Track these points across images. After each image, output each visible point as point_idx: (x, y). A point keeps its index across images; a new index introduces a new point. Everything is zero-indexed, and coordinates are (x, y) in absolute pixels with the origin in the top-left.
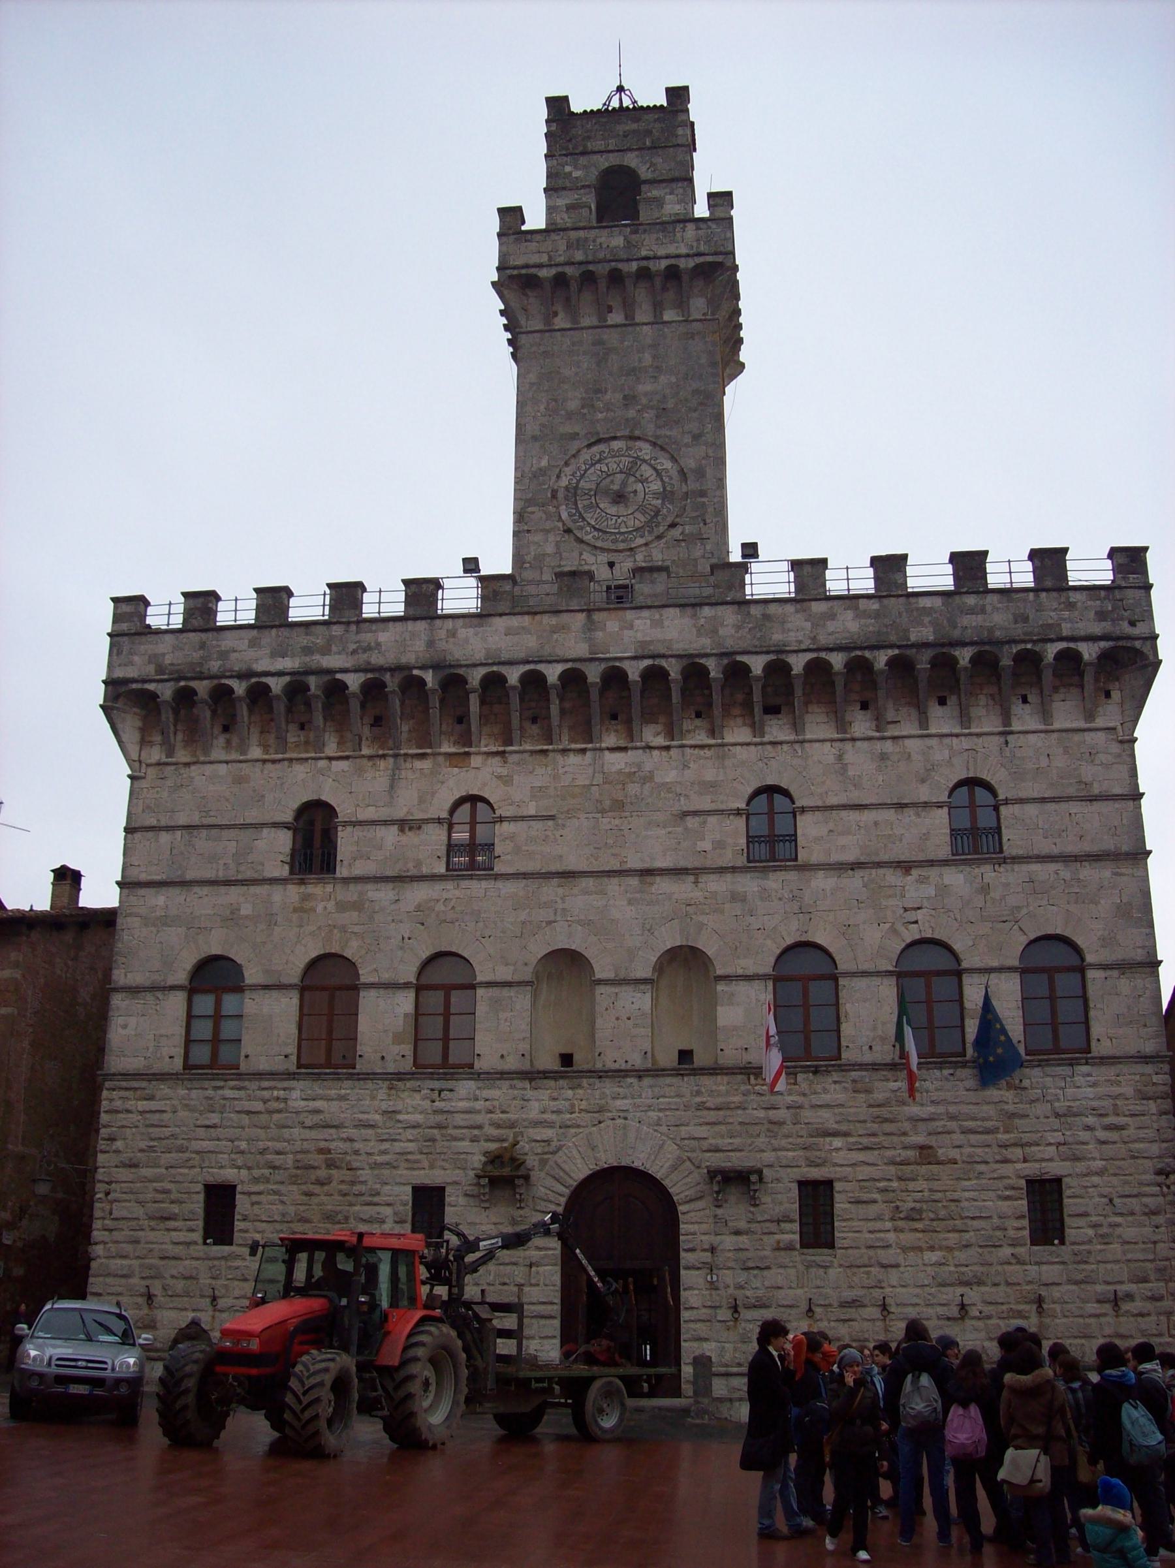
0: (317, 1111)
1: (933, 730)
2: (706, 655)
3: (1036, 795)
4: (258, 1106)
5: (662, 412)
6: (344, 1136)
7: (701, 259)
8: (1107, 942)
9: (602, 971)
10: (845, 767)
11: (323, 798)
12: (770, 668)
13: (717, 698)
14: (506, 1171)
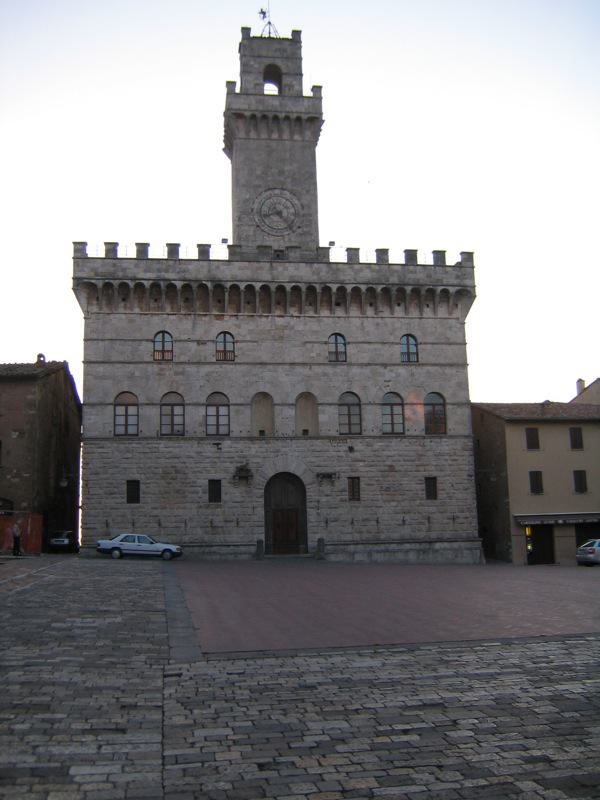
0: (170, 452)
4: (148, 451)
9: (277, 400)
10: (363, 328)
12: (338, 289)
13: (319, 298)
14: (243, 474)
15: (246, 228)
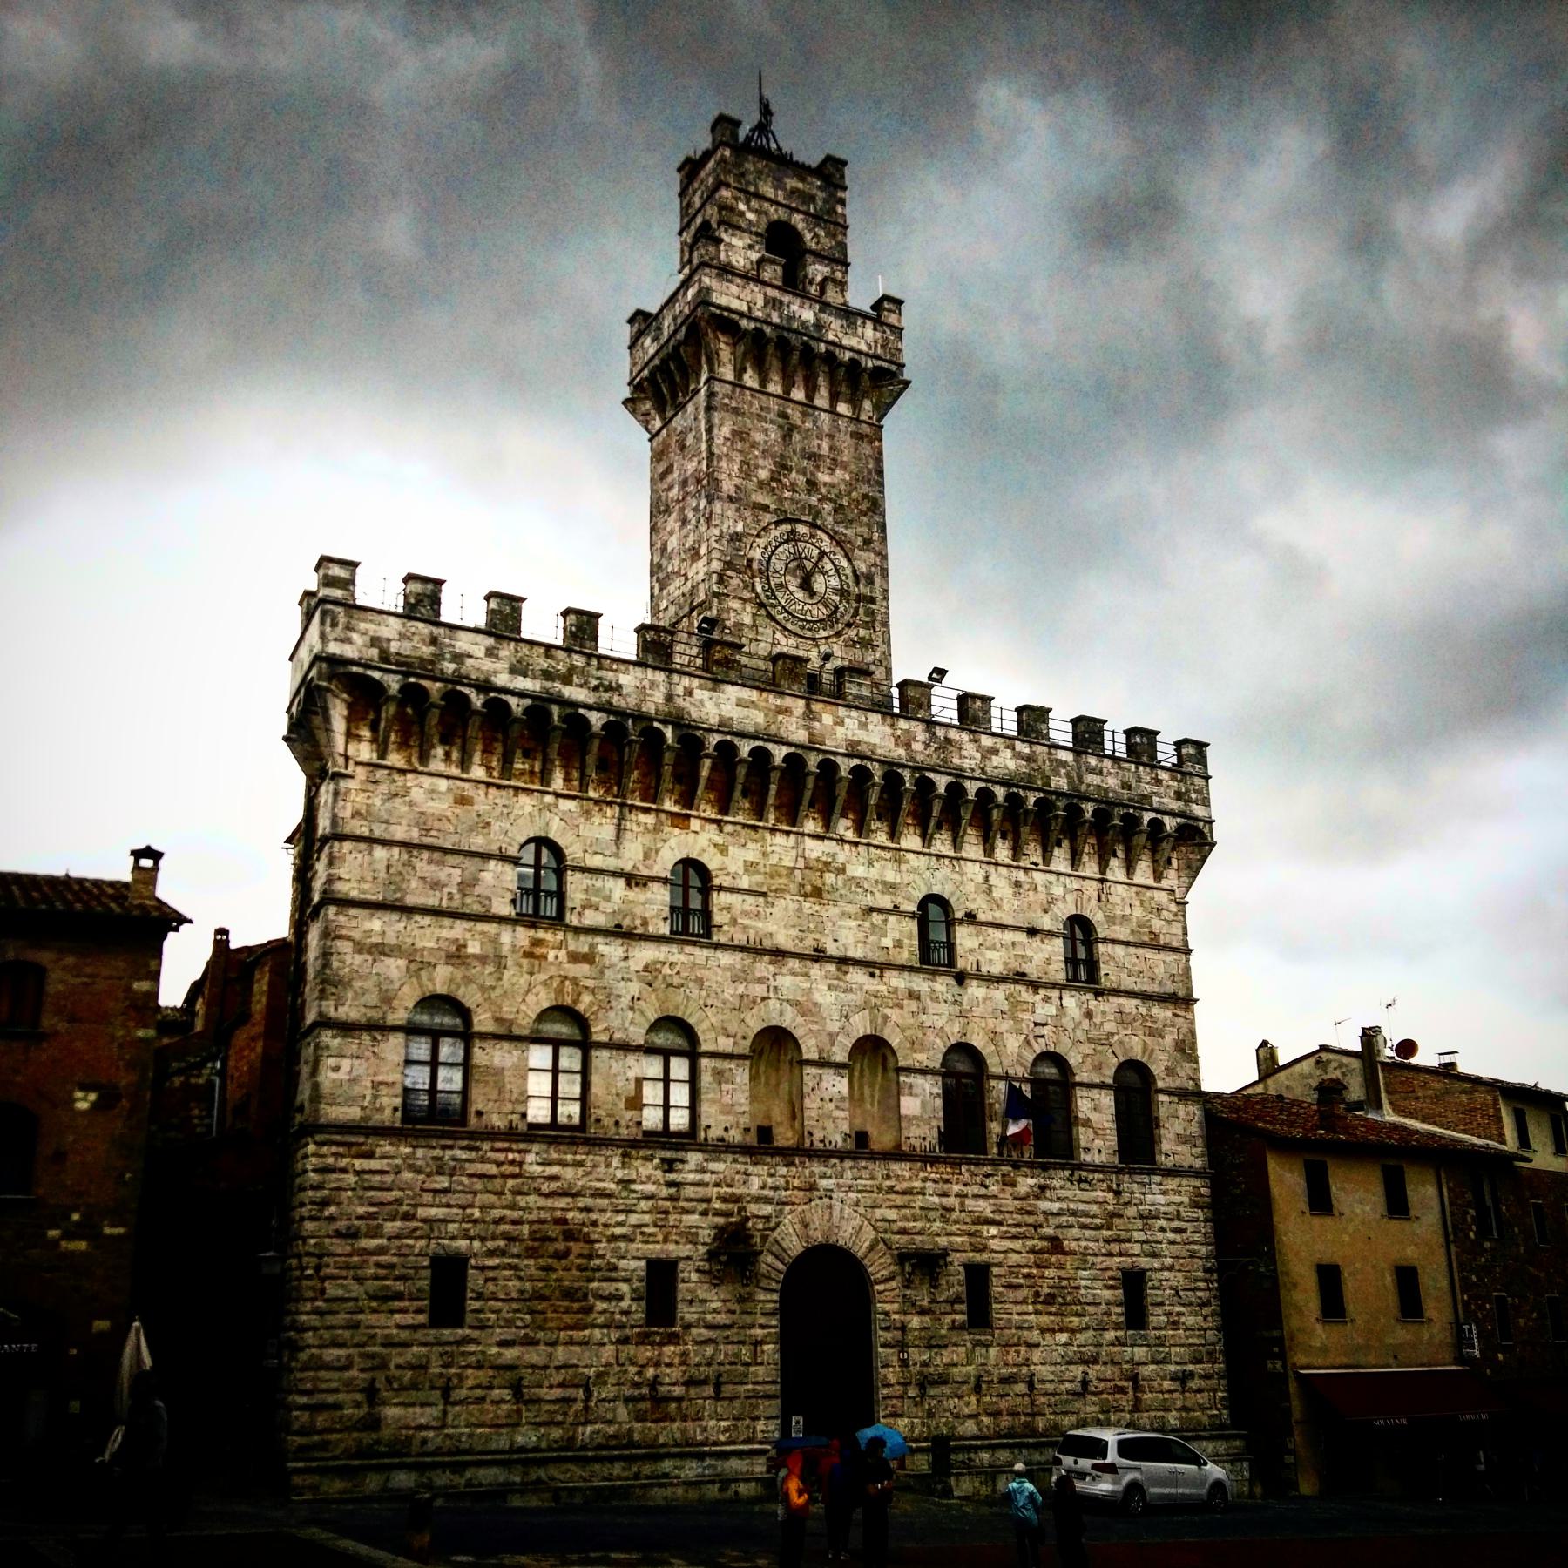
1: (1052, 867)
2: (904, 766)
3: (1122, 938)
4: (492, 1169)
5: (838, 509)
6: (581, 1205)
7: (879, 363)
8: (1170, 1071)
9: (809, 1050)
10: (989, 890)
11: (551, 836)
12: (949, 786)
15: (736, 605)
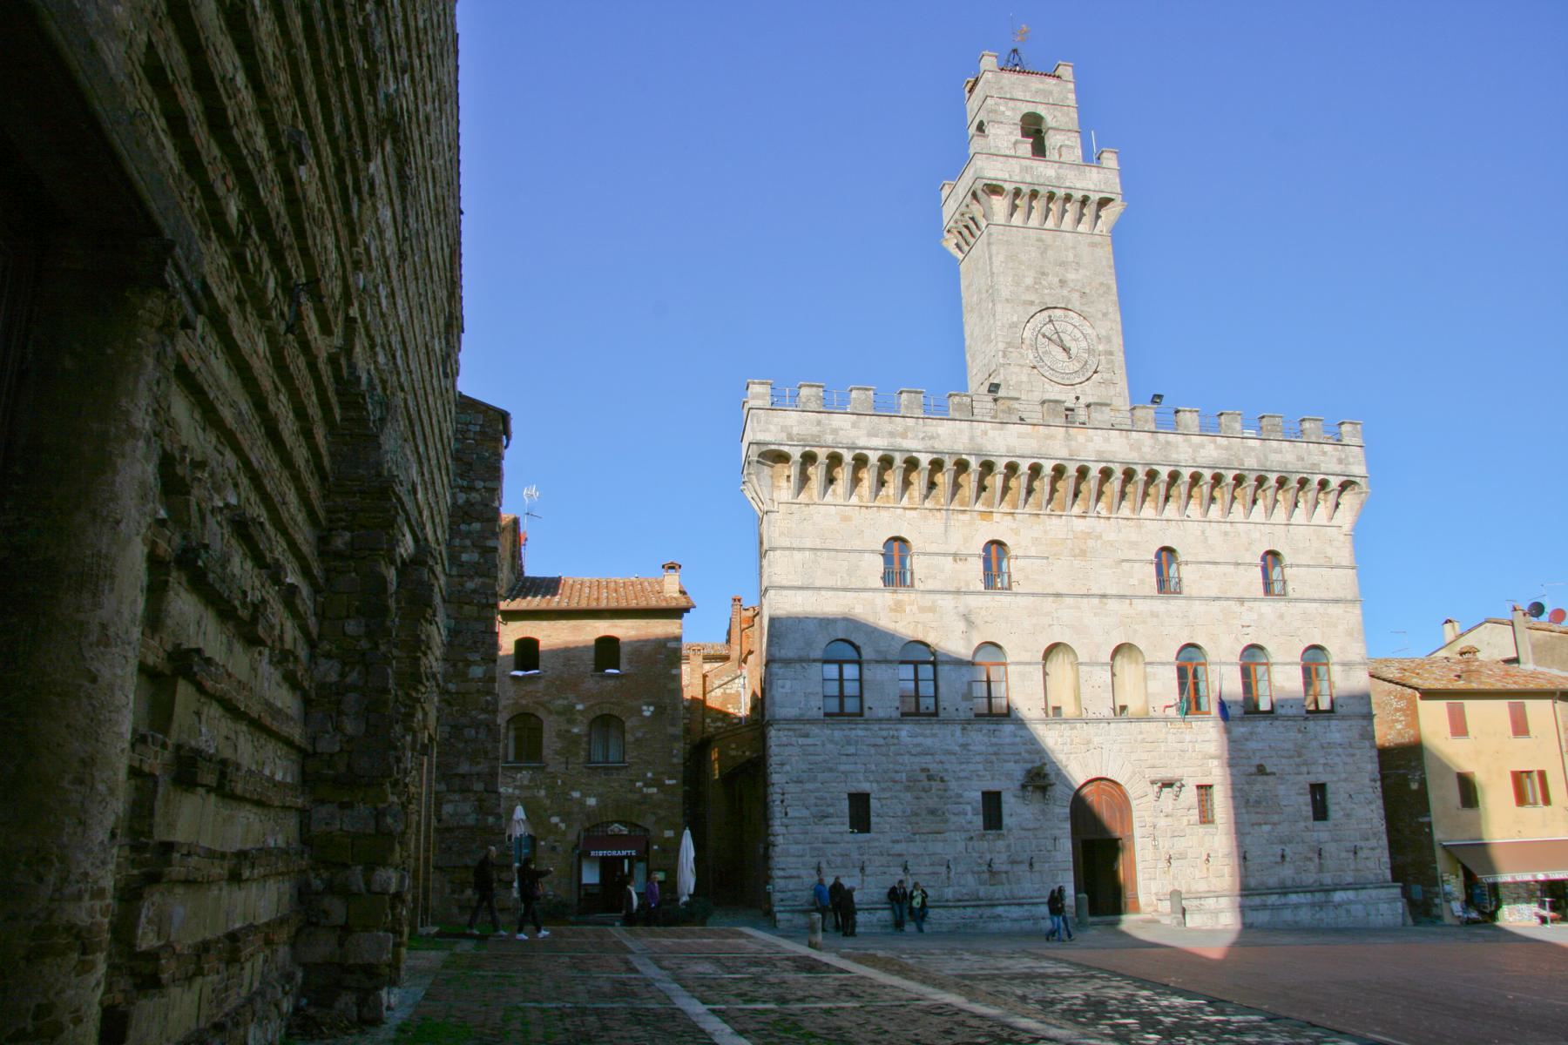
4: (881, 742)
10: (1206, 539)
15: (1017, 369)
